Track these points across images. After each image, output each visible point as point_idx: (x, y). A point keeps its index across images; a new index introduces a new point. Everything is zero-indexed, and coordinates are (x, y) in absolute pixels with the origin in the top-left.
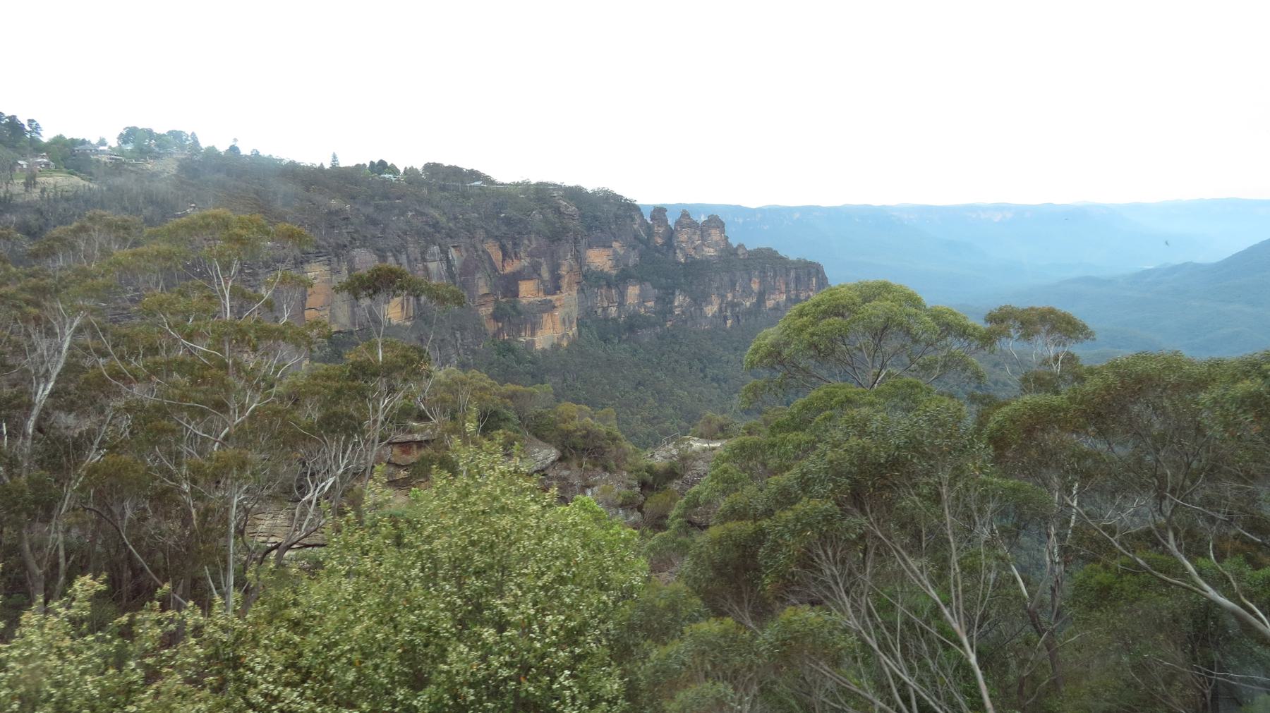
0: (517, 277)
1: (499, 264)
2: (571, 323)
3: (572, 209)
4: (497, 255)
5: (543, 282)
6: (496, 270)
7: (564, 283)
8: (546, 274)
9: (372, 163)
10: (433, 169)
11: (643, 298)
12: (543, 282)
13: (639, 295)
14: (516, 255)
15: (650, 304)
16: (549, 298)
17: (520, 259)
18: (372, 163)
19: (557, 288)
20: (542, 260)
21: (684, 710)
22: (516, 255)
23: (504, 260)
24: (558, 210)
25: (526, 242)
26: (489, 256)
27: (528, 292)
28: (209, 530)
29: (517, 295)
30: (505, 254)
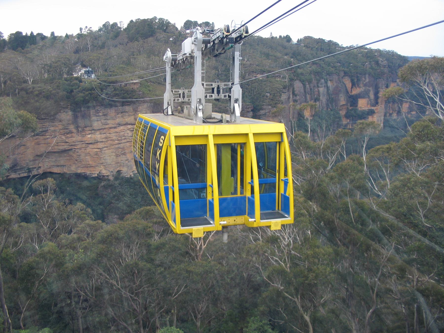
0: (359, 96)
1: (349, 90)
2: (381, 121)
3: (385, 62)
4: (348, 84)
5: (370, 100)
6: (348, 93)
7: (379, 100)
8: (372, 96)
9: (280, 37)
10: (308, 39)
11: (411, 109)
12: (370, 100)
13: (409, 108)
14: (358, 86)
15: (414, 113)
16: (372, 108)
17: (360, 87)
18: (280, 37)
19: (377, 103)
20: (371, 88)
21: (243, 313)
22: (358, 86)
23: (352, 88)
24: (377, 63)
25: (364, 79)
26: (346, 87)
27: (363, 104)
28: (129, 206)
29: (357, 106)
30: (353, 85)
